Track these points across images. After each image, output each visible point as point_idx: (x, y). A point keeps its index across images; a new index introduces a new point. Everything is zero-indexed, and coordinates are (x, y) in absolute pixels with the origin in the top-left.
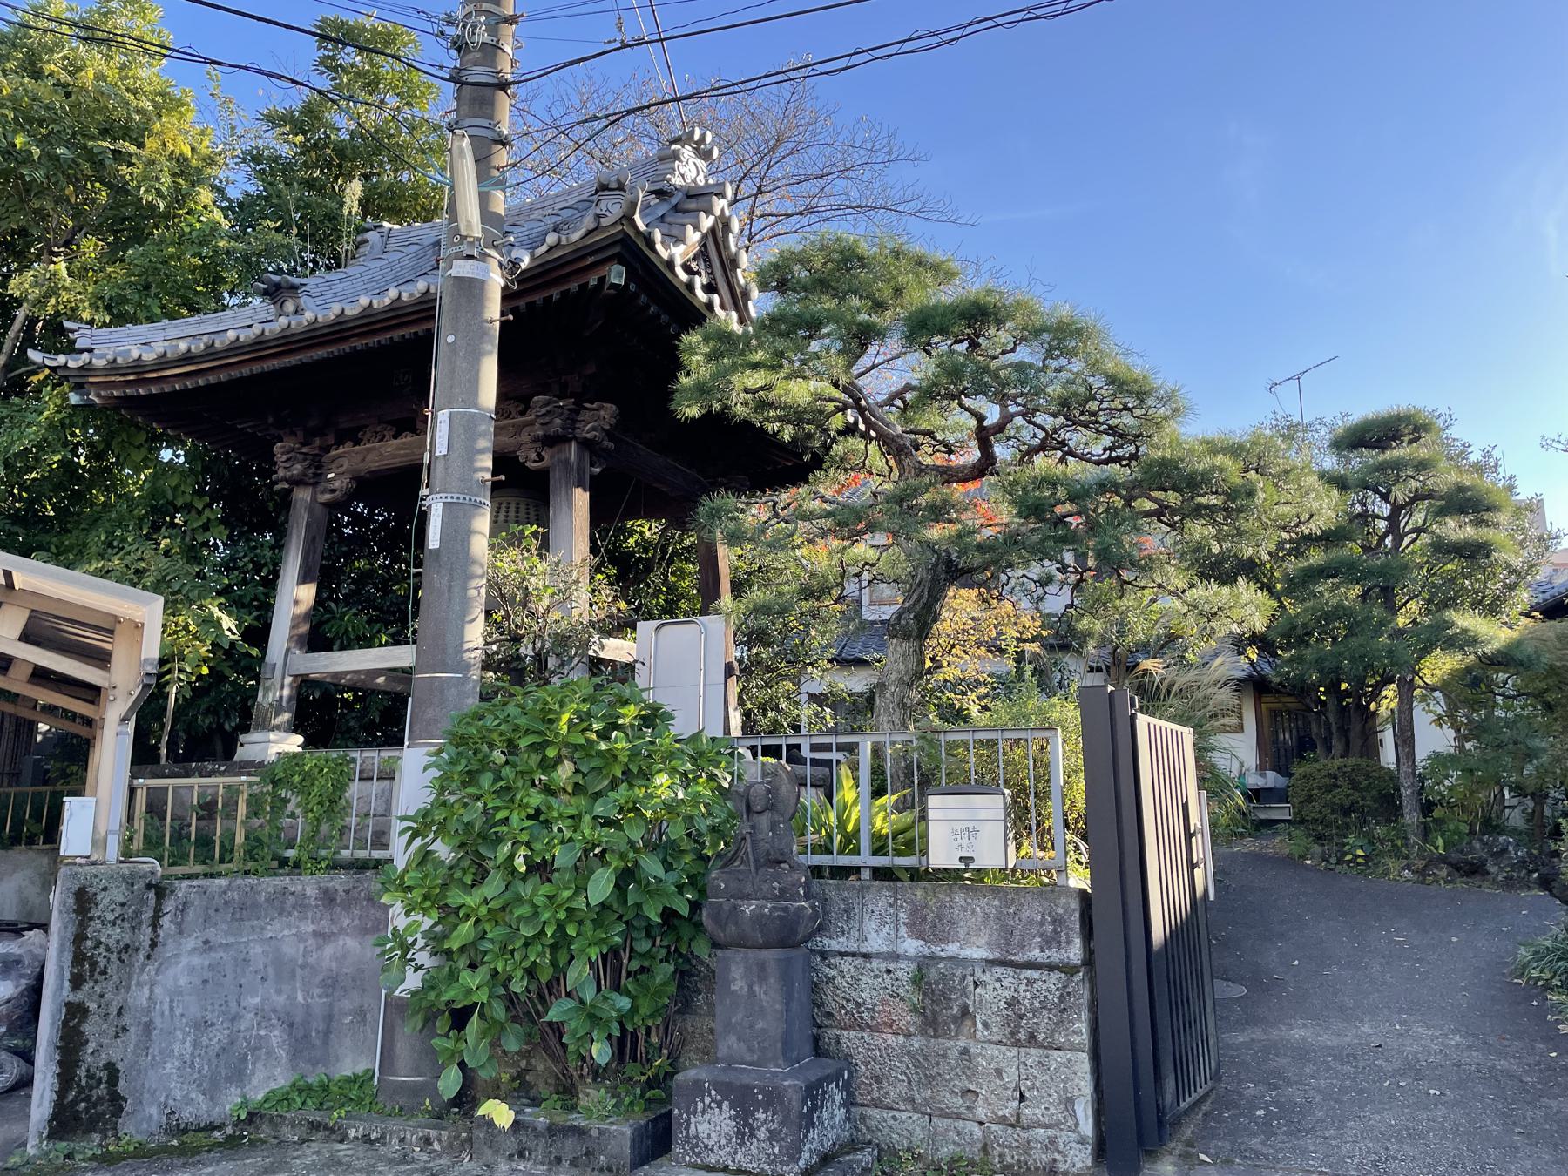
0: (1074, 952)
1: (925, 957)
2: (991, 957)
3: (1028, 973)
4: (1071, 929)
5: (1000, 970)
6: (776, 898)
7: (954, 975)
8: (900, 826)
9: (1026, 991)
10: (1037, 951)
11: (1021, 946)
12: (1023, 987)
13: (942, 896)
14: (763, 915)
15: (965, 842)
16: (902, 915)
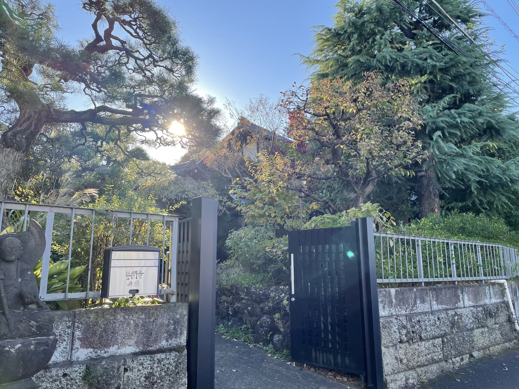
0: (183, 340)
1: (92, 359)
2: (137, 350)
3: (159, 356)
4: (183, 326)
5: (142, 358)
6: (34, 335)
7: (113, 367)
8: (54, 270)
9: (157, 367)
10: (164, 341)
11: (156, 341)
12: (156, 365)
13: (108, 317)
14: (29, 352)
15: (134, 280)
16: (78, 333)
